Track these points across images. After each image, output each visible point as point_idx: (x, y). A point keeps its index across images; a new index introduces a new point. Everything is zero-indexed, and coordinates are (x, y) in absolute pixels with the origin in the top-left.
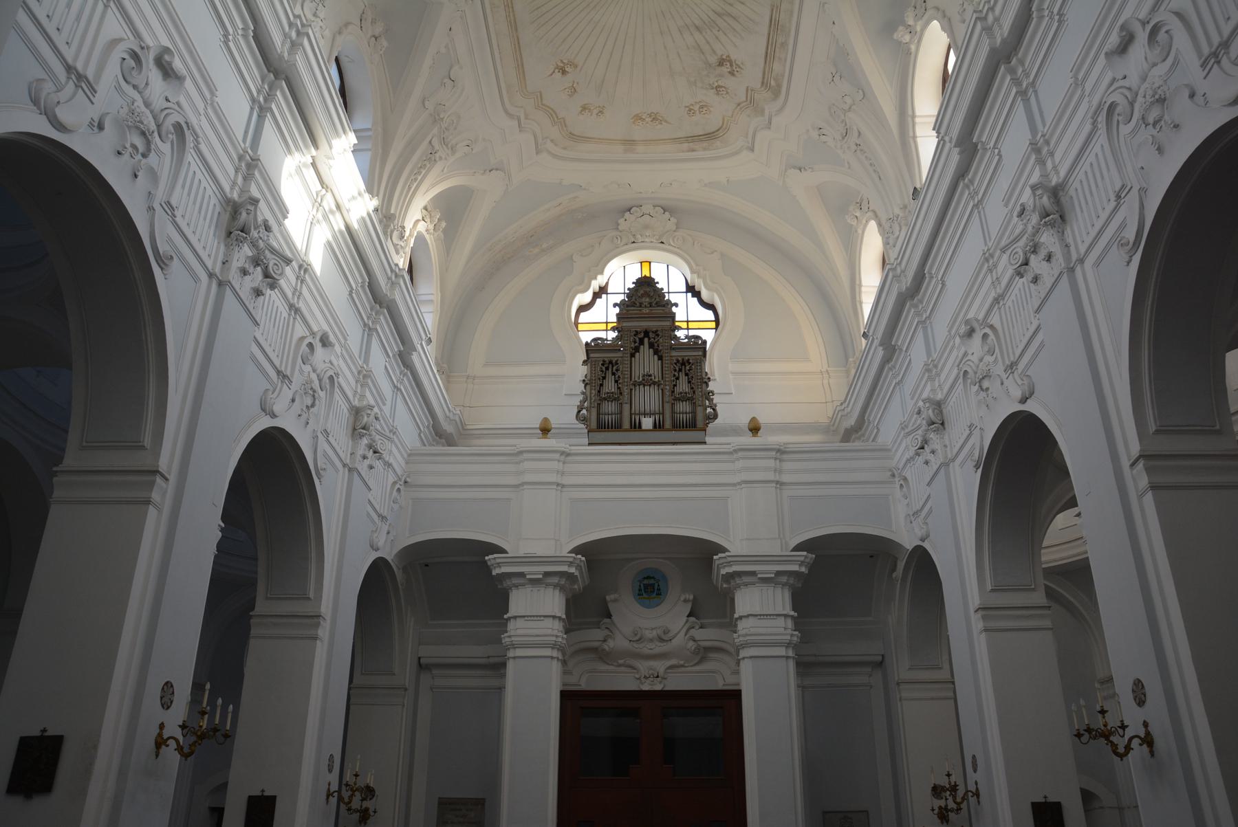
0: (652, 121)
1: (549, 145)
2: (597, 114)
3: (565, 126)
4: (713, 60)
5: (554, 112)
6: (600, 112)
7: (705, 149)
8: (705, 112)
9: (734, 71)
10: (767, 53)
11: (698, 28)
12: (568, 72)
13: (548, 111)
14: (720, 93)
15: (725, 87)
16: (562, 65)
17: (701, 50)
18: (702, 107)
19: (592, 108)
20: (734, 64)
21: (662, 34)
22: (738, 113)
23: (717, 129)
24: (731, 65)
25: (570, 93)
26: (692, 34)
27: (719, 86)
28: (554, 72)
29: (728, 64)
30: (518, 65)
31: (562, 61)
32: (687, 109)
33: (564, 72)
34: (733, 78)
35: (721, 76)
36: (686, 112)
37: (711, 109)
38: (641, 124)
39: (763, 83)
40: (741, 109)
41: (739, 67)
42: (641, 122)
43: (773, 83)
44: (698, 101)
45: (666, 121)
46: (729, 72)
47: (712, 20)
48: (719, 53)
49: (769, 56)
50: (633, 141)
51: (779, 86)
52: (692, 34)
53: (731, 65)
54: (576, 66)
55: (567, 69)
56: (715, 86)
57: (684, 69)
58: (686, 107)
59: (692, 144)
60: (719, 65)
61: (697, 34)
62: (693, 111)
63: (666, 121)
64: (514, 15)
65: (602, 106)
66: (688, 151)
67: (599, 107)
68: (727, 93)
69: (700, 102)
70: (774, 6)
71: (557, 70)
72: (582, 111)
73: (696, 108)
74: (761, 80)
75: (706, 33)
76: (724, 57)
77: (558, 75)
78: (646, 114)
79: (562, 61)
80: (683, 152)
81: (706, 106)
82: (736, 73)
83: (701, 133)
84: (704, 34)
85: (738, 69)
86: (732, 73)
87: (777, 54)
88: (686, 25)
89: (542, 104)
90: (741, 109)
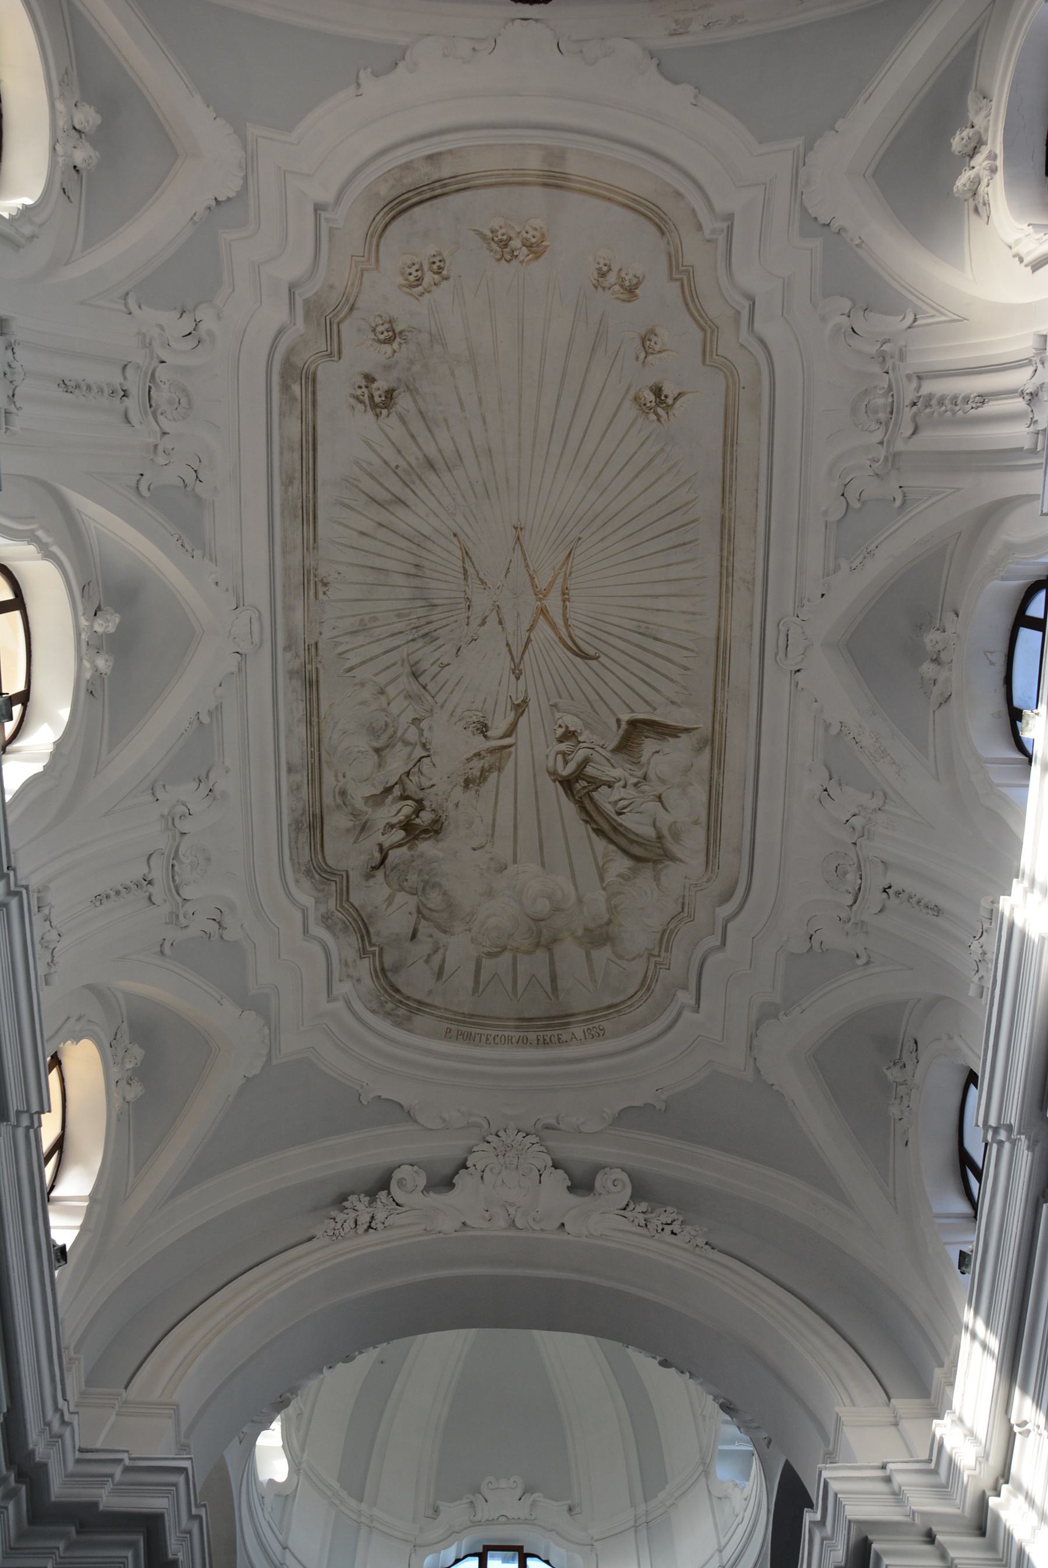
0: (510, 239)
1: (709, 225)
2: (610, 270)
3: (670, 256)
4: (404, 402)
5: (687, 305)
6: (603, 275)
7: (407, 166)
8: (413, 270)
9: (367, 387)
10: (315, 449)
11: (431, 465)
12: (651, 390)
13: (698, 311)
14: (387, 326)
15: (379, 341)
16: (659, 410)
17: (423, 418)
18: (419, 280)
19: (617, 288)
20: (367, 402)
21: (490, 451)
22: (352, 285)
23: (387, 232)
24: (372, 397)
25: (654, 339)
26: (440, 451)
27: (389, 341)
28: (675, 399)
29: (377, 399)
30: (732, 445)
31: (659, 420)
32: (444, 272)
33: (657, 391)
34: (367, 370)
35: (388, 368)
36: (447, 264)
37: (400, 280)
38: (532, 232)
39: (314, 381)
40: (348, 300)
41: (357, 398)
42: (529, 236)
43: (296, 388)
44: (427, 295)
45: (483, 237)
46: (373, 380)
47: (408, 486)
48: (394, 419)
49: (310, 444)
50: (545, 185)
51: (285, 388)
52: (440, 451)
53: (372, 397)
54: (636, 399)
55: (652, 398)
56: (398, 340)
57: (453, 374)
58: (447, 278)
59: (435, 177)
60: (393, 390)
61: (432, 451)
62: (435, 267)
63: (483, 237)
64: (721, 550)
65: (600, 289)
66: (440, 154)
67: (604, 288)
68: (374, 330)
69: (422, 294)
70: (314, 548)
71: (670, 401)
72: (637, 286)
73: (429, 278)
74: (318, 387)
75: (417, 459)
76: (385, 412)
77: (670, 390)
78: (521, 258)
79: (659, 420)
80: (450, 152)
81: (412, 286)
82: (363, 383)
83: (417, 210)
84: (421, 456)
85: (359, 392)
86: (369, 379)
87: (297, 456)
88: (450, 471)
89: (703, 330)
90: (348, 300)
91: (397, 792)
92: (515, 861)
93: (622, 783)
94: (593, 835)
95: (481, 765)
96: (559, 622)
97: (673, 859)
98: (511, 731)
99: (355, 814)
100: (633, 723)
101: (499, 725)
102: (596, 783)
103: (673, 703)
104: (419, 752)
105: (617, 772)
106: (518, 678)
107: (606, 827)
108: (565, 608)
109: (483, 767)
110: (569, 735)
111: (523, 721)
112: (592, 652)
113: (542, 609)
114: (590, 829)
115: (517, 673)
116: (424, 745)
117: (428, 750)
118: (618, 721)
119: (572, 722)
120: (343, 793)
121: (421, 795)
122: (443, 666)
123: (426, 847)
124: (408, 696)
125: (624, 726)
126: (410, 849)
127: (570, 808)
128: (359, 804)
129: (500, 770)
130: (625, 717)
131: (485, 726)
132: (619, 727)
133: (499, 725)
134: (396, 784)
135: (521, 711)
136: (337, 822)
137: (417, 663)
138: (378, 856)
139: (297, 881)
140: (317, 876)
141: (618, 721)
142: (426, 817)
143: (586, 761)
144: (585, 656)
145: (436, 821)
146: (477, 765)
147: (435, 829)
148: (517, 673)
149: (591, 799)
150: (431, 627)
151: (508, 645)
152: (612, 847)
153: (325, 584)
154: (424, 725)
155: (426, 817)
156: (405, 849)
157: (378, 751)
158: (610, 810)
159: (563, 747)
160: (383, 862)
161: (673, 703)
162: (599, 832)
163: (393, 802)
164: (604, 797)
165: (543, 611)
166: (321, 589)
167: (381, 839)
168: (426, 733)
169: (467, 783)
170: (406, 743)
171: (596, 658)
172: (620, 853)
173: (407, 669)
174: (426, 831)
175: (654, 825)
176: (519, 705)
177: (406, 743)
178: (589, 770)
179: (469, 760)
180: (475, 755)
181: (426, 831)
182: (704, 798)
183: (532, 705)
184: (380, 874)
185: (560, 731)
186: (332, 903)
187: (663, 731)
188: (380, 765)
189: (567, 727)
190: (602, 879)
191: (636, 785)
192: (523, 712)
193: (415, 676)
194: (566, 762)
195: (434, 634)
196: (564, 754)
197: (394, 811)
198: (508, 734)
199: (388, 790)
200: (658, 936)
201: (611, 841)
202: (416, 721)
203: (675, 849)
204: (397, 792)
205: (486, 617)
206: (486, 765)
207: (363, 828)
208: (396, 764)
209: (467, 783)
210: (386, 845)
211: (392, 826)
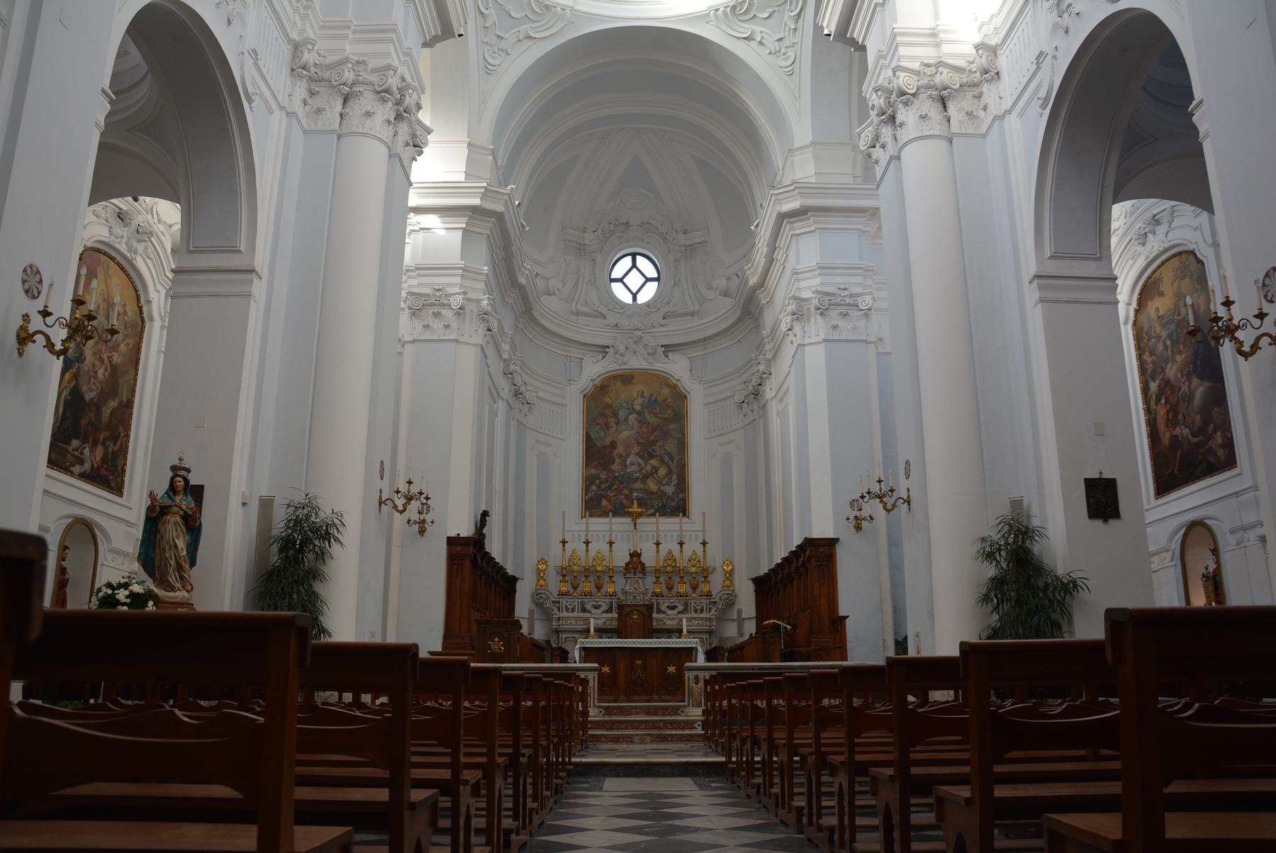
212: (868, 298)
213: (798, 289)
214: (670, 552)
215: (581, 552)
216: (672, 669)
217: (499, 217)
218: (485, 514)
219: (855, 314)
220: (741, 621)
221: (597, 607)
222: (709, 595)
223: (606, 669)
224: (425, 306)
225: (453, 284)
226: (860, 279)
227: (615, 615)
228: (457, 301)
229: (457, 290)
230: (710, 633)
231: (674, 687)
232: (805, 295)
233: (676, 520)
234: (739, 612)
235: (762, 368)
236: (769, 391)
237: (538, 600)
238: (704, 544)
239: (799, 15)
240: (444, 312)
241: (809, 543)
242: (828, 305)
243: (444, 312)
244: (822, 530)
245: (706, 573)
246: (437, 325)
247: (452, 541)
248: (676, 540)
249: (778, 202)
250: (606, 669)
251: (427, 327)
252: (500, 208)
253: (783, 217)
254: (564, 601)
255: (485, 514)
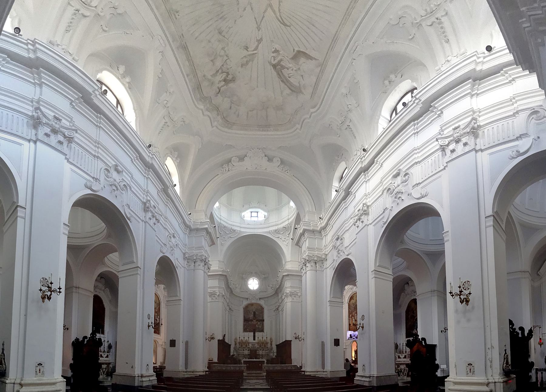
91: (220, 71)
92: (257, 87)
93: (292, 69)
94: (281, 82)
95: (246, 60)
96: (277, 10)
97: (303, 93)
98: (256, 49)
99: (209, 80)
100: (299, 52)
101: (252, 46)
102: (283, 67)
103: (313, 49)
104: (225, 58)
105: (291, 65)
106: (259, 31)
107: (285, 81)
108: (280, 5)
109: (247, 60)
110: (276, 51)
111: (260, 45)
112: (288, 24)
113: (270, 5)
114: (280, 81)
115: (259, 29)
116: (227, 56)
117: (228, 57)
118: (294, 50)
119: (277, 47)
120: (204, 76)
121: (228, 71)
122: (230, 28)
123: (231, 85)
124: (219, 41)
125: (295, 51)
126: (226, 86)
127: (274, 73)
128: (210, 77)
129: (253, 61)
130: (296, 49)
131: (247, 47)
132: (294, 51)
133: (252, 46)
134: (220, 69)
135: (260, 42)
136: (205, 84)
137: (220, 28)
138: (218, 90)
139: (198, 103)
140: (203, 100)
141: (294, 50)
142: (230, 77)
143: (281, 60)
144: (285, 25)
145: (233, 78)
146: (245, 60)
147: (233, 80)
148: (259, 29)
149: (282, 72)
150: (224, 14)
151: (255, 18)
152: (286, 86)
153: (177, 12)
154: (226, 49)
155: (230, 77)
156: (225, 86)
157: (212, 61)
158: (287, 76)
159: (274, 55)
160: (219, 91)
161: (313, 49)
162: (282, 81)
163: (220, 74)
164: (285, 72)
165: (270, 6)
166: (177, 14)
167: (218, 85)
168: (227, 52)
169: (242, 66)
170: (221, 56)
171: (290, 26)
172: (288, 88)
173: (217, 31)
174: (231, 81)
175: (299, 83)
176: (259, 40)
177: (221, 56)
178: (282, 63)
179: (242, 58)
180: (244, 57)
181: (231, 81)
182: (315, 80)
183: (264, 40)
184: (219, 95)
185: (273, 50)
186: (208, 105)
187: (308, 57)
188: (213, 64)
189: (276, 48)
190: (282, 93)
191: (296, 70)
192: (261, 43)
193: (220, 33)
194: (274, 60)
195: (225, 16)
196: (274, 57)
197: (220, 77)
198: (255, 49)
199: (217, 71)
200: (295, 111)
201: (286, 84)
202: (223, 49)
203: (303, 91)
204: (220, 71)
205: (246, 8)
206: (248, 60)
207: (212, 83)
208: (219, 63)
209: (242, 66)
210: (220, 87)
211: (220, 81)
212: (300, 294)
213: (286, 291)
214: (260, 340)
215: (243, 339)
216: (260, 365)
217: (226, 276)
218: (225, 335)
219: (297, 296)
220: (273, 353)
221: (246, 350)
222: (268, 347)
223: (248, 365)
224: (212, 295)
225: (217, 290)
226: (299, 290)
227: (250, 351)
228: (218, 294)
229: (218, 291)
230: (268, 355)
231: (260, 368)
232: (288, 292)
233: (261, 333)
234: (273, 351)
235: (279, 304)
236: (280, 309)
237: (234, 348)
238: (267, 338)
239: (289, 234)
240: (215, 296)
241: (286, 341)
242: (292, 294)
243: (215, 296)
244: (289, 339)
245: (267, 343)
246: (214, 298)
247: (218, 340)
248: (261, 337)
249: (283, 273)
250: (248, 365)
251: (212, 299)
252: (225, 274)
253: (284, 276)
254: (240, 349)
255: (225, 335)
